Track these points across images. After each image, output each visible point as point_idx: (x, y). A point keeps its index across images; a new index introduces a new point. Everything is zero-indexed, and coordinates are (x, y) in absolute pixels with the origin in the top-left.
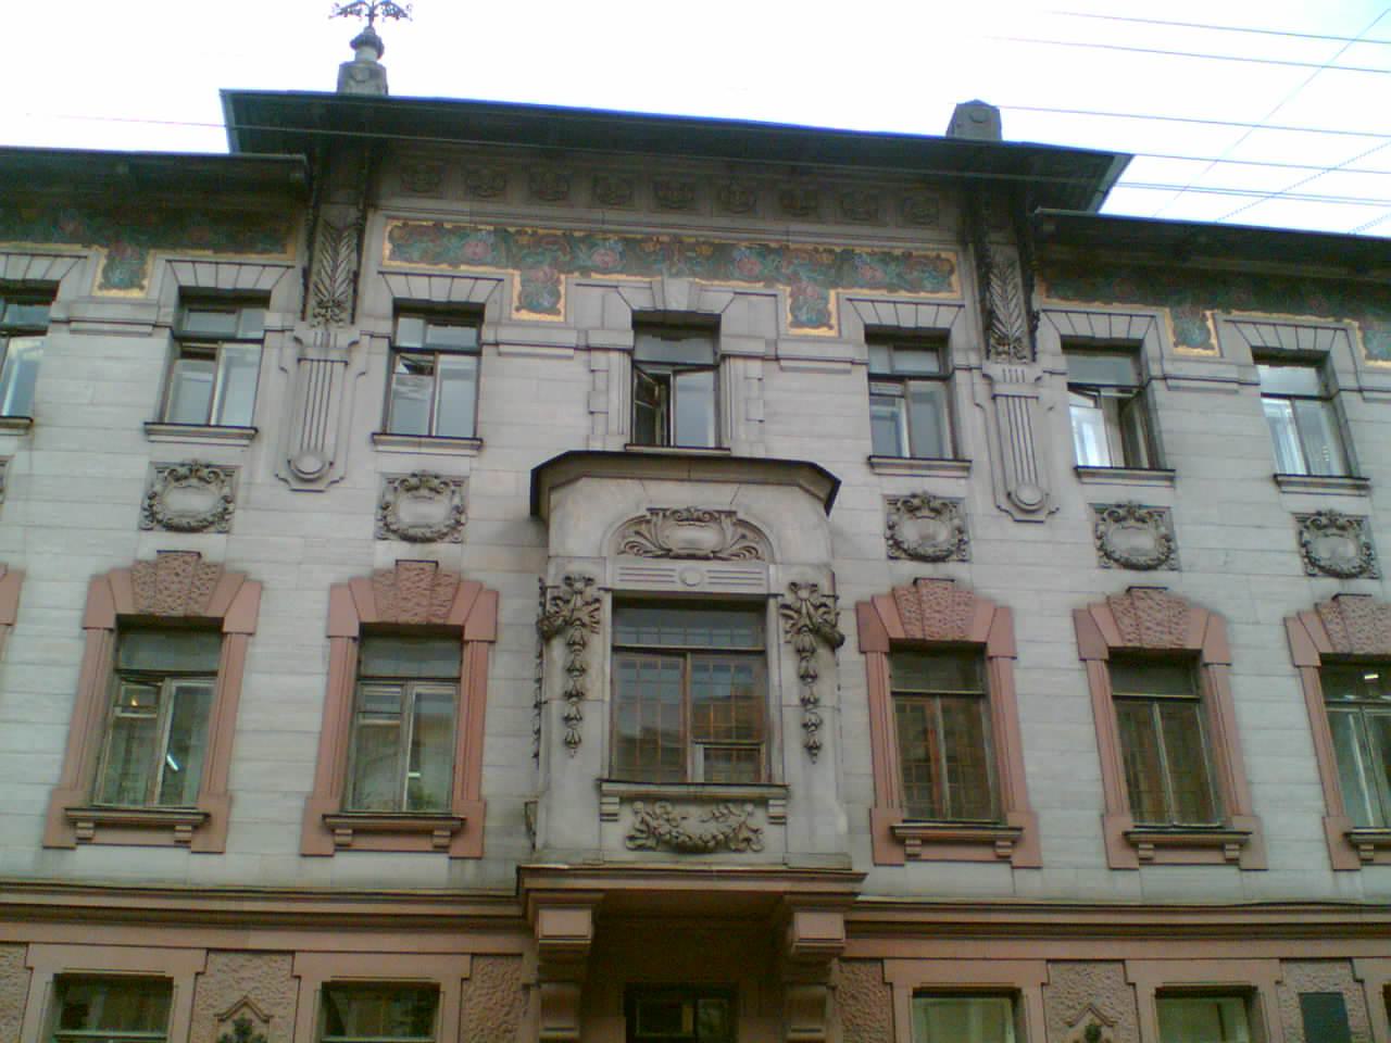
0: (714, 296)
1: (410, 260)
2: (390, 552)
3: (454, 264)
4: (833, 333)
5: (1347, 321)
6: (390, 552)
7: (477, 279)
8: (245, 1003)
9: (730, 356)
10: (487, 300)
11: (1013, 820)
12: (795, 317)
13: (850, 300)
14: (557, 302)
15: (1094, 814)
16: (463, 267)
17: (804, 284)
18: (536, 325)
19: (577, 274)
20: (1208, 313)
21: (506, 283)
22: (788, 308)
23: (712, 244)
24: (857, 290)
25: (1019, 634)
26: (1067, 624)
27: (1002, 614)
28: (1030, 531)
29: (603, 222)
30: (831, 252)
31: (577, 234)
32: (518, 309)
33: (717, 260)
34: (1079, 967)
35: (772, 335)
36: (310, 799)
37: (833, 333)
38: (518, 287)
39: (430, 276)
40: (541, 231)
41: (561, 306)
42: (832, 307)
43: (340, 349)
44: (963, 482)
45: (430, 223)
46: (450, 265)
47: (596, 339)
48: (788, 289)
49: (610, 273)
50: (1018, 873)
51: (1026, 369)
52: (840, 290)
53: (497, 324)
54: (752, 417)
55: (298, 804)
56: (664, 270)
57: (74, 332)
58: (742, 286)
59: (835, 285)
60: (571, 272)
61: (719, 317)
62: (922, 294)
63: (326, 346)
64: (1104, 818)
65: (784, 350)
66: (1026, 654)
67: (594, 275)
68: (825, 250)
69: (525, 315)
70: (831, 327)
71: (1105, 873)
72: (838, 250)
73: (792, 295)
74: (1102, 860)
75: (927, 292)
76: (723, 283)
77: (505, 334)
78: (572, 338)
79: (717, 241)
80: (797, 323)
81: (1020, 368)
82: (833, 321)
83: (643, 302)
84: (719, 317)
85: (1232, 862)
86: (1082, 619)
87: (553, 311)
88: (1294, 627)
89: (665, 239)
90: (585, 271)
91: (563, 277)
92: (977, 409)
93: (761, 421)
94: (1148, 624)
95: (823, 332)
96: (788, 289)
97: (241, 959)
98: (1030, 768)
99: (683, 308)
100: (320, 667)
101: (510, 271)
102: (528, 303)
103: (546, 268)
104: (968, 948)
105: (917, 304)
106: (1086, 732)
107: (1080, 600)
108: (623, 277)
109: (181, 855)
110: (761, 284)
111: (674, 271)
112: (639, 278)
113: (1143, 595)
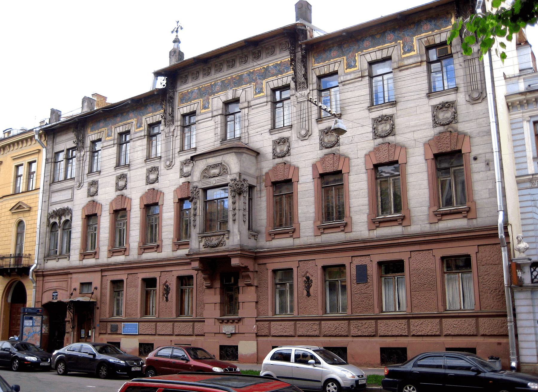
0: (239, 92)
2: (183, 180)
5: (399, 41)
6: (183, 180)
8: (166, 282)
11: (294, 226)
12: (256, 92)
15: (312, 222)
16: (192, 101)
20: (356, 54)
21: (200, 103)
23: (239, 76)
24: (269, 78)
25: (300, 174)
26: (310, 169)
27: (297, 169)
28: (305, 142)
29: (217, 78)
30: (264, 68)
31: (213, 83)
33: (239, 81)
34: (306, 262)
36: (173, 239)
40: (206, 85)
44: (290, 131)
45: (186, 91)
50: (295, 239)
51: (305, 91)
52: (266, 80)
55: (171, 240)
57: (133, 141)
58: (244, 86)
62: (284, 74)
63: (169, 132)
64: (314, 222)
65: (252, 103)
66: (301, 179)
67: (216, 94)
69: (204, 111)
71: (313, 237)
72: (265, 67)
74: (312, 234)
79: (240, 74)
81: (304, 92)
83: (224, 99)
85: (343, 231)
86: (314, 166)
88: (368, 157)
89: (229, 78)
94: (328, 165)
97: (165, 273)
98: (299, 212)
100: (173, 210)
102: (205, 108)
104: (282, 259)
106: (312, 199)
107: (314, 161)
109: (156, 253)
110: (248, 85)
113: (327, 157)
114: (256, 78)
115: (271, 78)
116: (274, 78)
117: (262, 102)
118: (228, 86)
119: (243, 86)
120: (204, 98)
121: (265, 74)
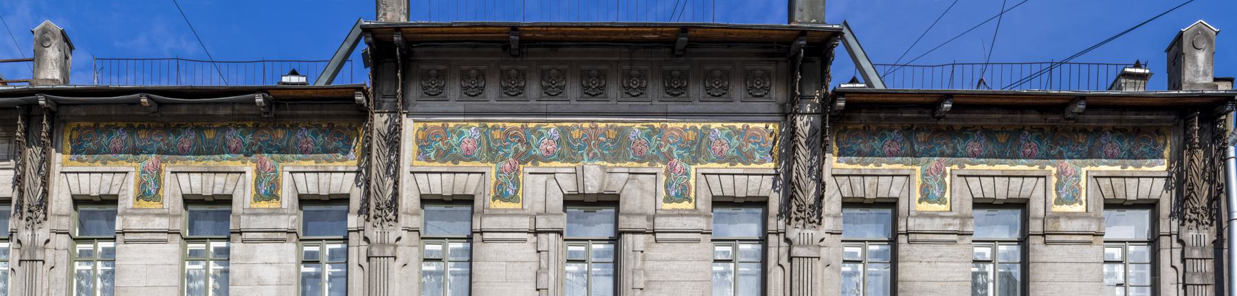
1: (428, 159)
3: (456, 161)
16: (461, 163)
52: (699, 165)
62: (753, 165)
69: (499, 205)
73: (667, 173)
87: (514, 199)
90: (535, 159)
91: (521, 166)
99: (595, 191)
102: (501, 195)
108: (559, 164)
111: (591, 155)
114: (670, 151)
119: (628, 164)
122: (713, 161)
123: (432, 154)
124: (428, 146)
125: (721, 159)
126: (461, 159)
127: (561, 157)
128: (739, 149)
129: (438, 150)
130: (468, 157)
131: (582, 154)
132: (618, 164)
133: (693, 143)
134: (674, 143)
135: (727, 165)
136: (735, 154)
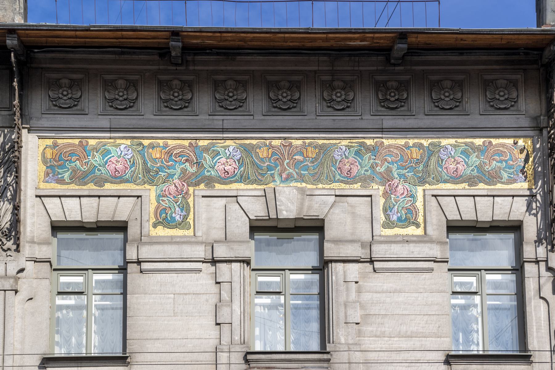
1: (61, 181)
3: (100, 182)
4: (419, 232)
7: (119, 197)
9: (331, 261)
10: (129, 216)
12: (387, 217)
13: (435, 196)
14: (185, 217)
16: (108, 186)
17: (396, 181)
18: (172, 241)
19: (202, 186)
22: (381, 208)
32: (155, 226)
35: (367, 237)
37: (419, 232)
38: (154, 204)
39: (80, 197)
41: (190, 219)
42: (419, 204)
43: (10, 277)
46: (95, 184)
47: (221, 252)
48: (382, 188)
49: (231, 182)
52: (427, 186)
53: (140, 242)
54: (350, 320)
56: (277, 178)
59: (422, 181)
60: (197, 184)
61: (323, 220)
62: (499, 186)
67: (218, 186)
68: (414, 145)
69: (161, 231)
70: (418, 225)
73: (386, 195)
75: (503, 183)
76: (328, 186)
77: (146, 252)
78: (200, 252)
80: (388, 224)
82: (420, 219)
84: (323, 220)
87: (182, 224)
90: (210, 182)
91: (191, 189)
92: (541, 301)
93: (357, 324)
95: (411, 230)
96: (382, 188)
99: (292, 216)
101: (147, 186)
103: (176, 181)
105: (494, 196)
108: (242, 186)
111: (284, 176)
112: (254, 186)
114: (389, 171)
115: (449, 186)
116: (461, 188)
117: (416, 255)
118: (269, 168)
119: (335, 185)
120: (164, 187)
121: (427, 166)
122: (446, 181)
123: (66, 176)
124: (61, 166)
125: (456, 179)
126: (107, 181)
127: (244, 179)
128: (480, 168)
129: (75, 171)
130: (117, 178)
131: (272, 176)
132: (320, 186)
133: (418, 162)
134: (392, 163)
135: (465, 185)
136: (475, 173)
